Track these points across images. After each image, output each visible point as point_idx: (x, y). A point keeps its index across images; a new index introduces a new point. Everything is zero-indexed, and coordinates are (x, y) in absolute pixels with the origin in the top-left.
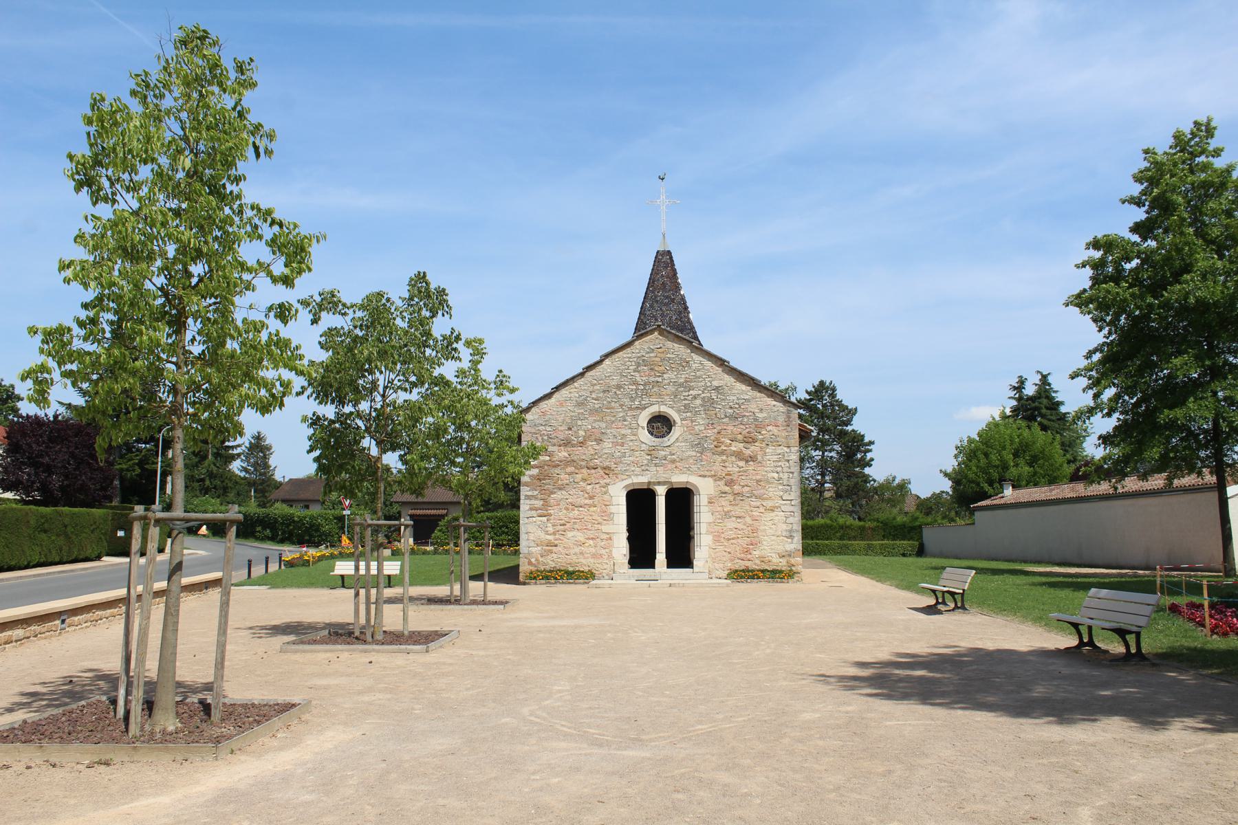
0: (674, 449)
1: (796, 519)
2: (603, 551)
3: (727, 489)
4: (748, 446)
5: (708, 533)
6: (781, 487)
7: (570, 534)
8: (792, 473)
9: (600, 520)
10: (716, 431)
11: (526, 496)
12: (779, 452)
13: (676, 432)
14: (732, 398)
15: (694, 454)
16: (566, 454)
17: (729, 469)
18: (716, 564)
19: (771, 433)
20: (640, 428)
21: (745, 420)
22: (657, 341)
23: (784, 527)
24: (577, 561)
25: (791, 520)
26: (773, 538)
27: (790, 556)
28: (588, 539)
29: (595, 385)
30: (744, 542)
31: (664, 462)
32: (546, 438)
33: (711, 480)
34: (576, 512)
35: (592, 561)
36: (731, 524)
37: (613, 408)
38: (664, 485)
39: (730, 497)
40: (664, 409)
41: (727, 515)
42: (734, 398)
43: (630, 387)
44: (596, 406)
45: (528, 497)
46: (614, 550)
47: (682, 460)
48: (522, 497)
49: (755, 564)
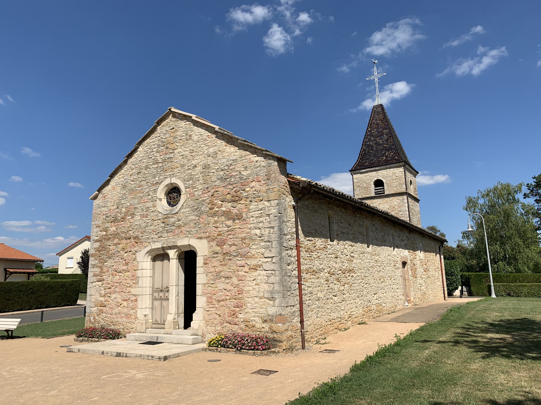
0: (181, 215)
1: (277, 278)
2: (132, 312)
3: (219, 248)
4: (235, 204)
5: (204, 294)
6: (262, 244)
7: (113, 296)
8: (272, 228)
9: (131, 284)
10: (210, 194)
11: (92, 265)
12: (261, 207)
13: (183, 198)
14: (224, 160)
15: (194, 217)
16: (114, 228)
17: (220, 229)
18: (209, 327)
19: (254, 189)
20: (158, 200)
21: (233, 180)
22: (171, 123)
23: (266, 287)
24: (116, 320)
25: (272, 279)
26: (257, 299)
27: (272, 320)
28: (123, 300)
29: (133, 169)
30: (231, 303)
31: (173, 228)
32: (104, 217)
33: (205, 241)
34: (117, 277)
35: (124, 319)
36: (221, 286)
37: (142, 186)
38: (174, 249)
39: (220, 257)
40: (174, 180)
41: (218, 276)
42: (224, 160)
43: (154, 166)
44: (133, 186)
45: (94, 266)
46: (138, 310)
47: (185, 224)
48: (90, 266)
49: (241, 328)
